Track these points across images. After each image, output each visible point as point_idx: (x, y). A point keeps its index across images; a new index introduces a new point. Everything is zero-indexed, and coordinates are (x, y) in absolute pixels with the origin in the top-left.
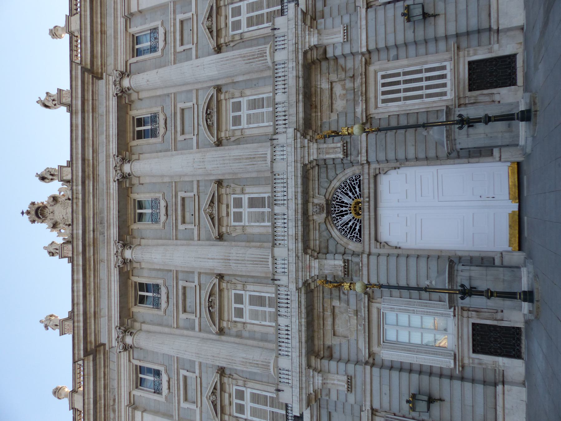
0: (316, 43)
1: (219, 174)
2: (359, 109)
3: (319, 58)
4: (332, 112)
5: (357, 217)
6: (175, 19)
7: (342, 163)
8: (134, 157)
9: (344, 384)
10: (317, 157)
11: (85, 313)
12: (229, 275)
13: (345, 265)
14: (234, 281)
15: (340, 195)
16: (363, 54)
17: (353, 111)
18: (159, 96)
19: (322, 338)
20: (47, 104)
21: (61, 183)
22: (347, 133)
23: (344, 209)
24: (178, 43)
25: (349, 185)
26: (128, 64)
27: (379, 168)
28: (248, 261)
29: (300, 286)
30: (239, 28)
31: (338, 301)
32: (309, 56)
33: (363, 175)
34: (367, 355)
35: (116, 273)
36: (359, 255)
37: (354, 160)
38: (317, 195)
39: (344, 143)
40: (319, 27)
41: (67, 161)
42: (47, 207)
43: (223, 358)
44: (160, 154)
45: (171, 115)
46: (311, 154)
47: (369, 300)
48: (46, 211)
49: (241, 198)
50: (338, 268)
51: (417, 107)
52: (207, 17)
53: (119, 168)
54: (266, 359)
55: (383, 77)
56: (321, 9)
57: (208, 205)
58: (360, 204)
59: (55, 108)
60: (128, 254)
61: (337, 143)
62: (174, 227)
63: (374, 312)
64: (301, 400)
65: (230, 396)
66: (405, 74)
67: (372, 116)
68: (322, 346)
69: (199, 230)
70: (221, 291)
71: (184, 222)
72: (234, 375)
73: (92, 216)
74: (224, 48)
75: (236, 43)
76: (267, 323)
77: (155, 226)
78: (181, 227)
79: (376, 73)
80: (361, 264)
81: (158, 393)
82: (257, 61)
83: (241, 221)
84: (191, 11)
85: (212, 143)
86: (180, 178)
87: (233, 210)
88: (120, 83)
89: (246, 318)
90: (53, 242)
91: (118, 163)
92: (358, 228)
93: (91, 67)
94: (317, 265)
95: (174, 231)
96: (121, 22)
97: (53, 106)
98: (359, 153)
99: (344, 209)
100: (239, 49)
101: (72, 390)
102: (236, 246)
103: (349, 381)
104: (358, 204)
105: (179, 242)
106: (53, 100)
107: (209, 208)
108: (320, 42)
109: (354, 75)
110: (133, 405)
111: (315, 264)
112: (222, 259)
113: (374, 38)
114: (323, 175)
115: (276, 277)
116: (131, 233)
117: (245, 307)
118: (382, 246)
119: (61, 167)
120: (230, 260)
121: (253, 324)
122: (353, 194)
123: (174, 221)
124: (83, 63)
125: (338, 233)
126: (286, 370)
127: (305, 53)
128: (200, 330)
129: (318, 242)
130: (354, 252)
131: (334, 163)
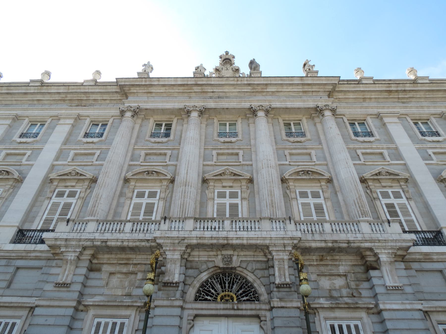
0: (381, 259)
1: (258, 180)
3: (367, 263)
4: (318, 275)
5: (219, 298)
6: (383, 148)
7: (271, 283)
9: (64, 280)
10: (276, 259)
12: (173, 187)
13: (173, 284)
14: (168, 191)
15: (240, 282)
16: (377, 305)
17: (320, 296)
18: (319, 138)
19: (109, 262)
20: (306, 66)
21: (249, 74)
22: (302, 278)
23: (227, 285)
24: (364, 151)
25: (250, 290)
27: (266, 321)
28: (184, 201)
29: (158, 241)
32: (368, 253)
34: (86, 303)
35: (180, 106)
36: (182, 297)
37: (273, 294)
38: (240, 259)
39: (289, 285)
40: (396, 263)
42: (231, 66)
43: (104, 180)
44: (273, 137)
45: (305, 146)
46: (278, 253)
47: (139, 307)
48: (228, 66)
49: (237, 198)
50: (171, 276)
52: (389, 171)
53: (261, 108)
54: (98, 214)
55: (356, 327)
56: (413, 267)
57: (232, 171)
58: (231, 301)
59: (303, 71)
60: (194, 114)
61: (290, 278)
62: (215, 147)
64: (56, 239)
65: (73, 186)
67: (317, 314)
68: (102, 262)
69: (211, 165)
70: (161, 180)
71: (218, 154)
72: (90, 190)
73: (224, 91)
75: (370, 194)
77: (216, 134)
79: (360, 319)
80: (174, 299)
81: (85, 136)
82: (357, 210)
83: (218, 197)
85: (284, 175)
86: (254, 152)
87: (228, 191)
88: (327, 109)
89: (136, 200)
90: (205, 70)
92: (209, 298)
93: (337, 91)
94: (176, 257)
96: (375, 111)
97: (305, 69)
98: (281, 299)
99: (227, 285)
100: (367, 197)
102: (197, 193)
103: (65, 285)
104: (231, 299)
105: (202, 150)
106: (309, 69)
107: (230, 172)
109: (355, 297)
111: (177, 256)
112: (186, 180)
113: (394, 317)
114: (258, 266)
115: (167, 221)
116: (210, 118)
118: (189, 321)
119: (261, 73)
120: (185, 186)
121: (130, 206)
122: (241, 294)
123: (219, 147)
124: (340, 86)
126: (85, 229)
127: (371, 249)
128: (130, 165)
129: (197, 259)
130: (186, 293)
131: (270, 275)
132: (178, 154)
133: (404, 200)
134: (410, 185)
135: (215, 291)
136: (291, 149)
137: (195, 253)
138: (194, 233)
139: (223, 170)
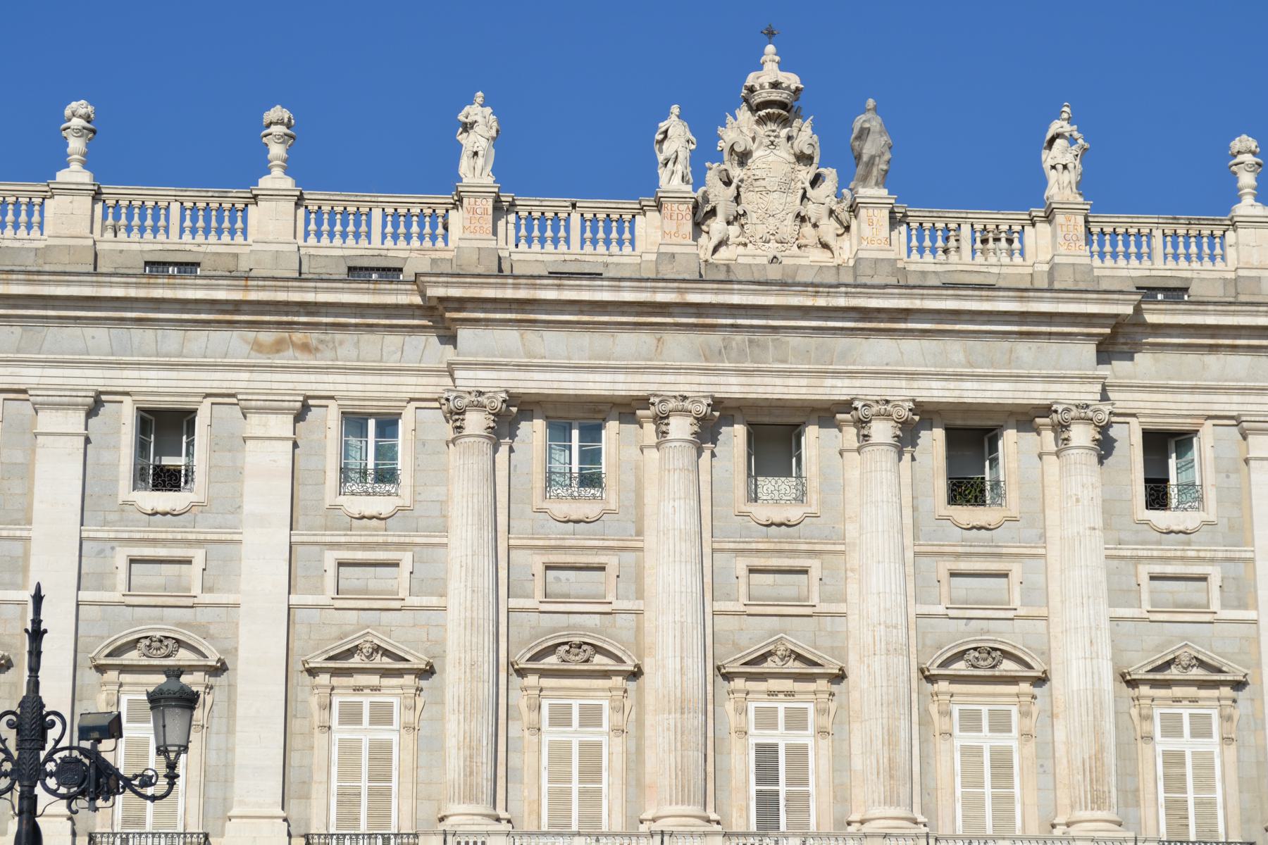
6: (1212, 560)
24: (1158, 569)
26: (1127, 419)
30: (1166, 732)
35: (633, 387)
49: (806, 728)
57: (793, 648)
65: (376, 689)
76: (545, 785)
78: (741, 564)
84: (1224, 606)
87: (781, 706)
95: (732, 546)
117: (576, 732)
121: (540, 751)
123: (754, 546)
133: (1212, 744)
136: (958, 556)
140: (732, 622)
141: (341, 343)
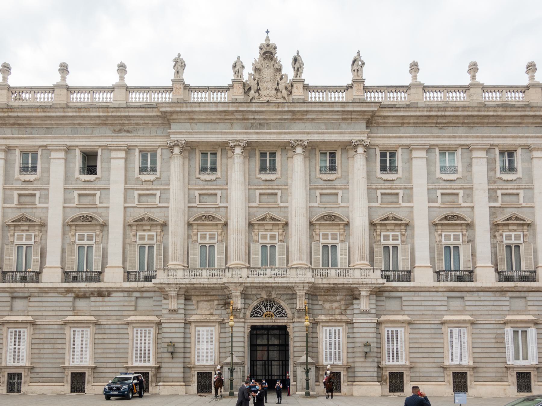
0: (362, 294)
2: (323, 317)
5: (264, 315)
6: (400, 189)
8: (307, 153)
11: (193, 112)
16: (352, 320)
19: (195, 294)
23: (269, 308)
29: (226, 285)
30: (384, 240)
31: (217, 304)
33: (287, 319)
38: (277, 293)
41: (308, 84)
42: (272, 60)
51: (321, 347)
55: (339, 330)
59: (352, 70)
60: (238, 150)
63: (214, 324)
65: (149, 230)
66: (339, 342)
68: (191, 294)
69: (255, 207)
70: (217, 225)
74: (373, 228)
78: (257, 192)
79: (342, 326)
91: (303, 142)
92: (258, 315)
95: (255, 187)
99: (269, 308)
101: (128, 85)
102: (246, 236)
108: (362, 297)
110: (128, 150)
111: (238, 293)
114: (288, 297)
122: (277, 313)
123: (261, 187)
125: (255, 305)
128: (189, 207)
129: (250, 293)
132: (227, 194)
134: (408, 228)
135: (262, 311)
136: (322, 189)
137: (249, 290)
138: (248, 279)
139: (264, 215)
140: (254, 210)
141: (139, 130)
